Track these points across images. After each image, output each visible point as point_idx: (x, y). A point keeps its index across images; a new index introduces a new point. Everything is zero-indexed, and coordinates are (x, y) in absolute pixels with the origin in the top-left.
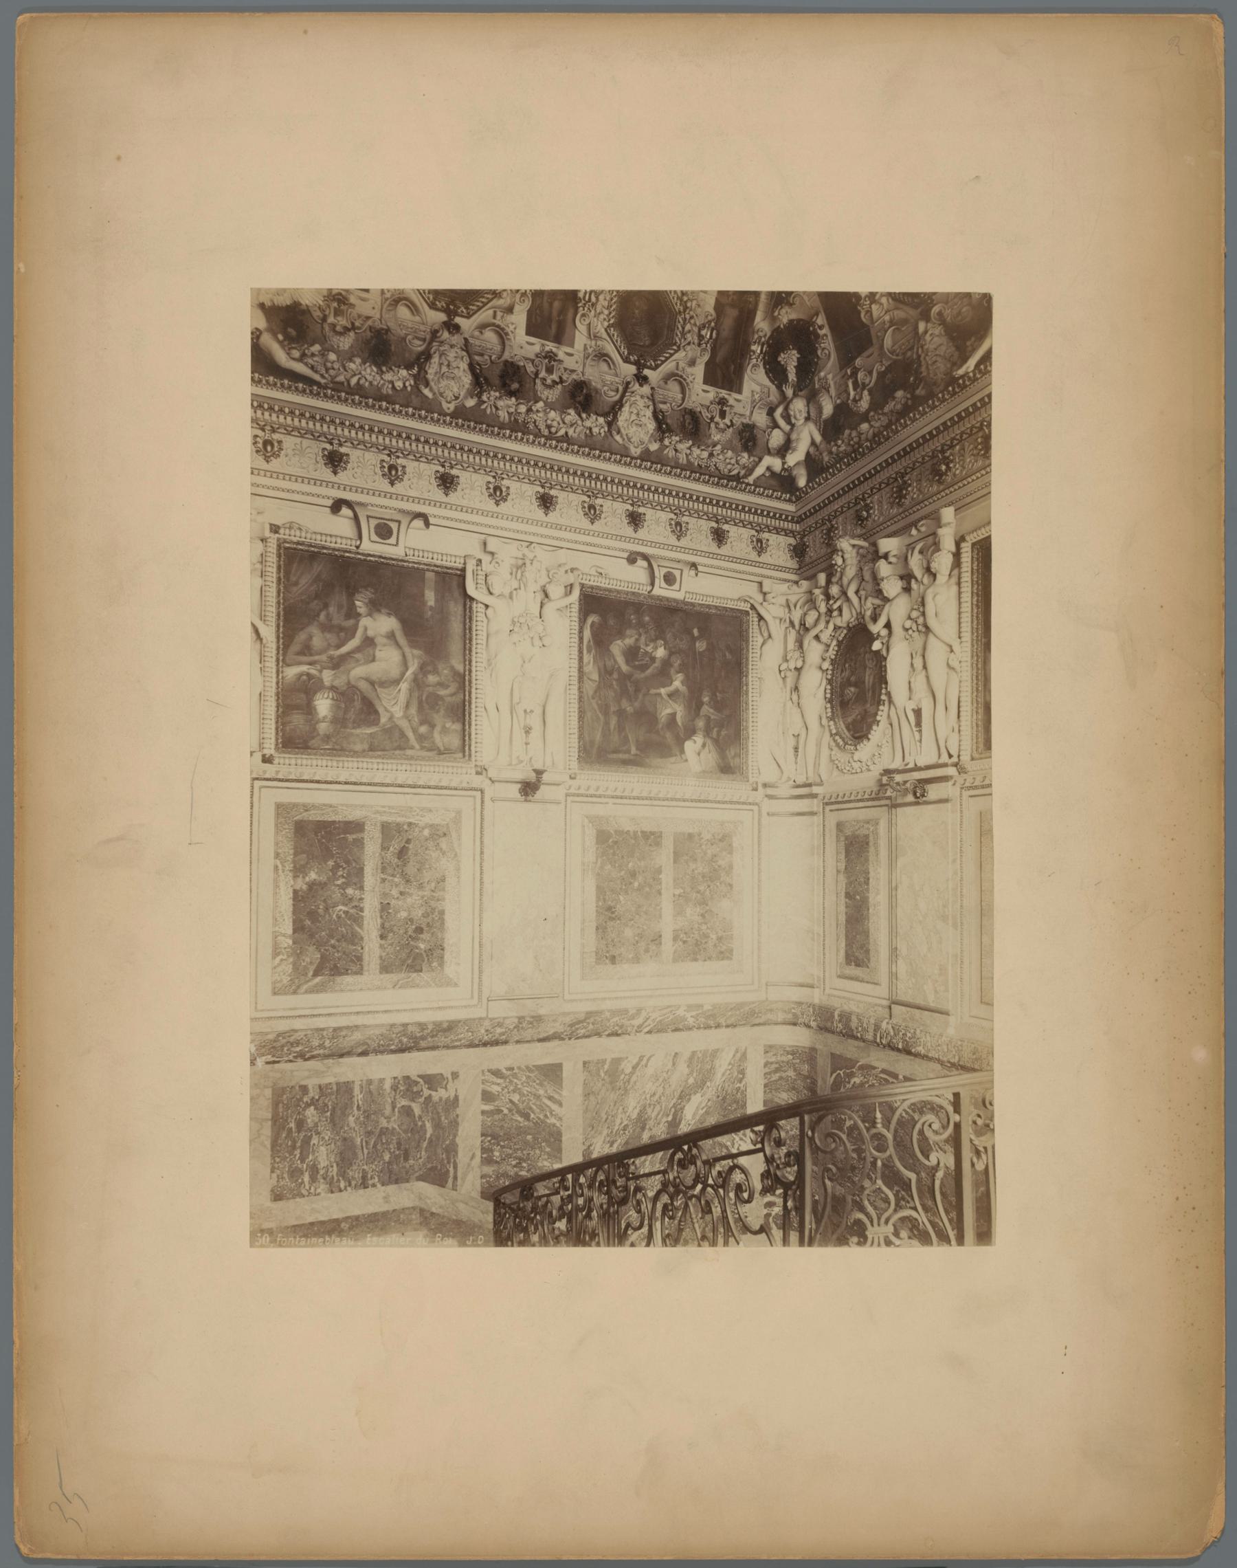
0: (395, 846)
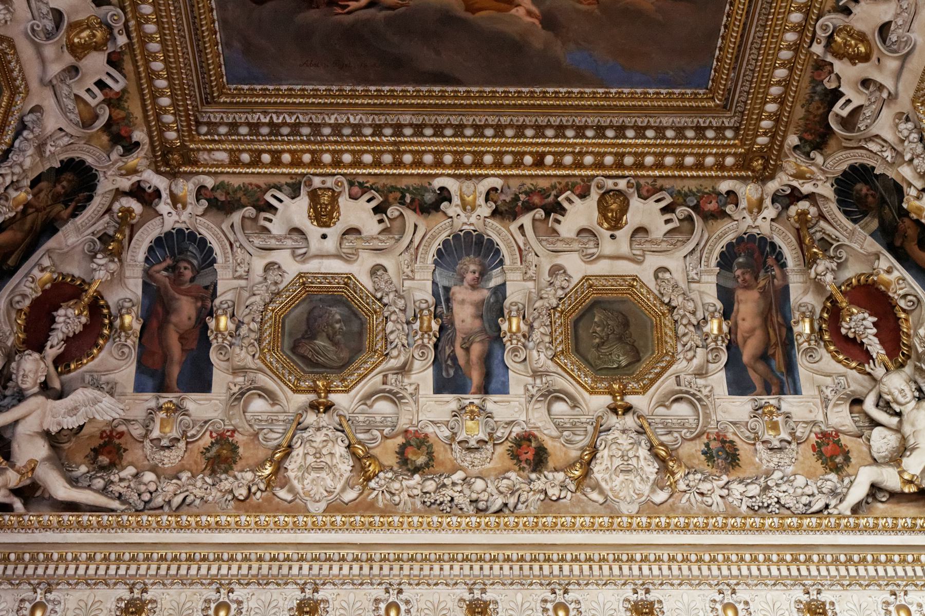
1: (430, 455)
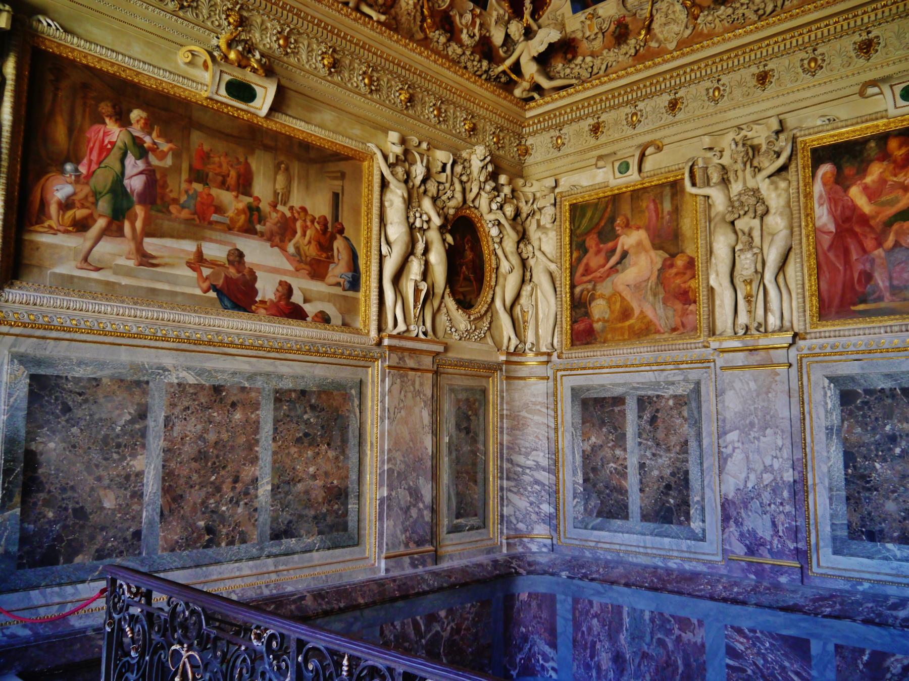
0: (647, 416)
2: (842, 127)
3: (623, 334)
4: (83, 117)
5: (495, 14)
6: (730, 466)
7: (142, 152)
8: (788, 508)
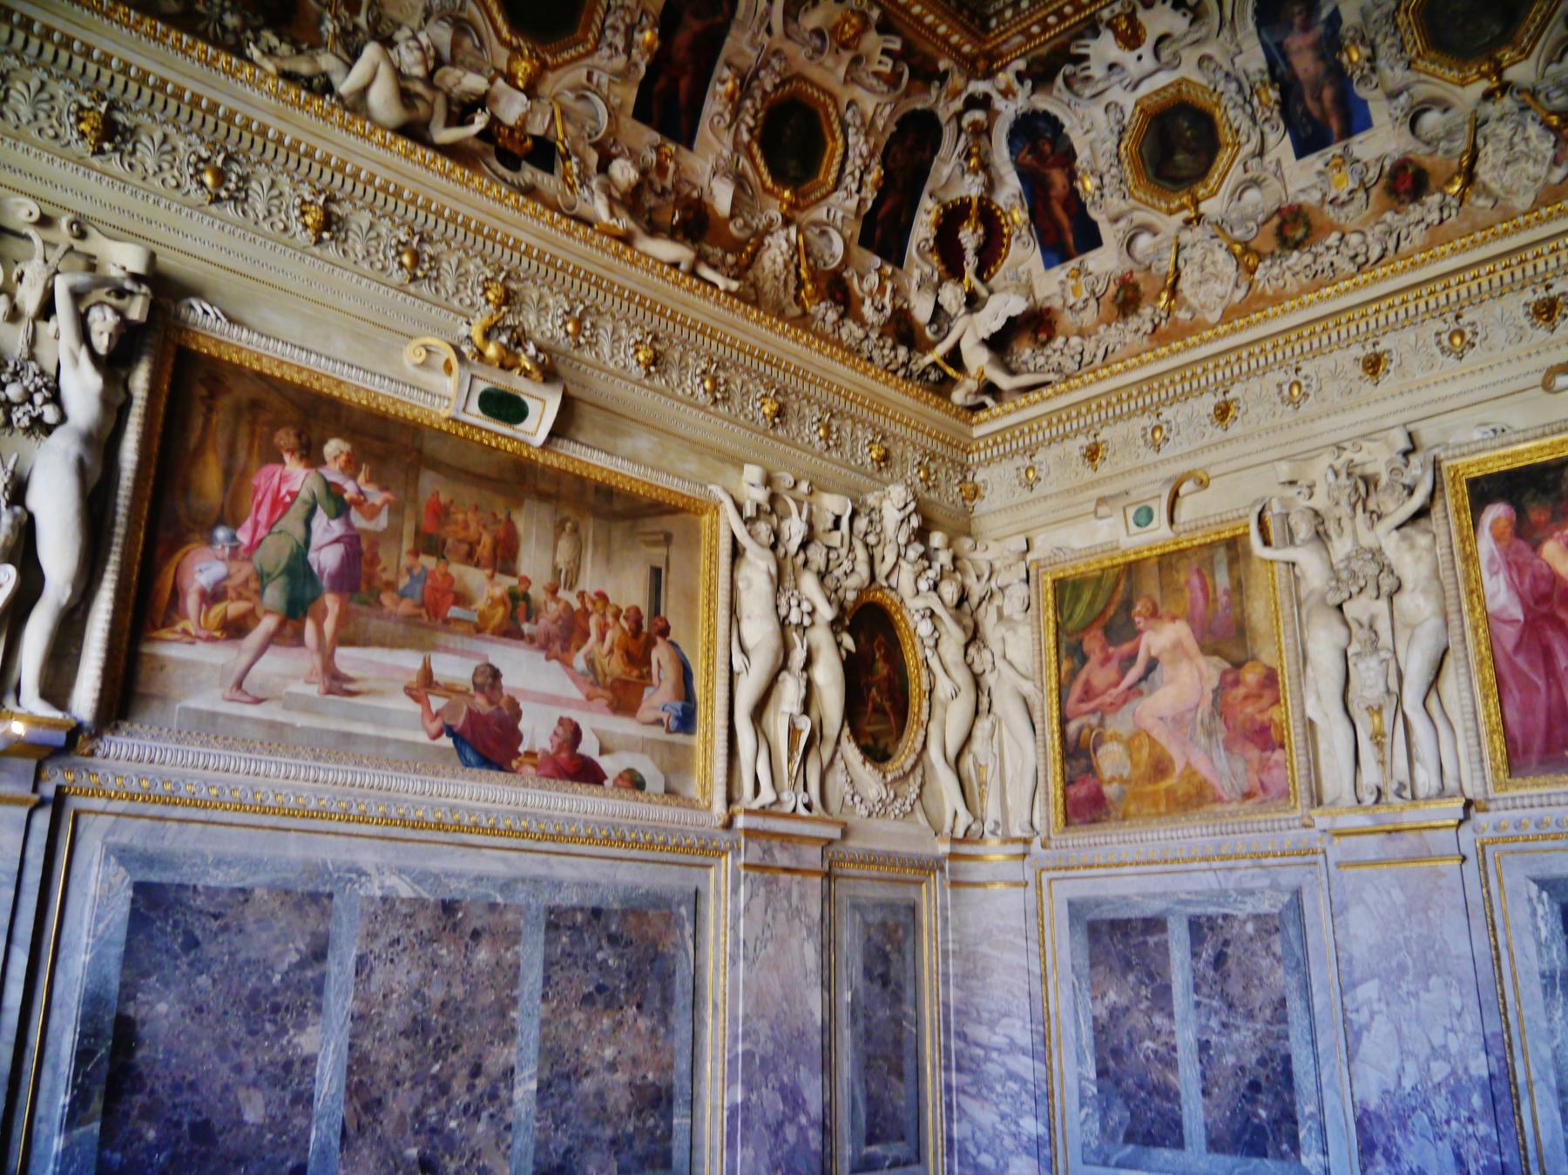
0: (1208, 953)
1: (1308, 225)
2: (1519, 442)
3: (1156, 804)
4: (250, 453)
5: (916, 274)
6: (1367, 1046)
7: (340, 505)
8: (1483, 1128)
